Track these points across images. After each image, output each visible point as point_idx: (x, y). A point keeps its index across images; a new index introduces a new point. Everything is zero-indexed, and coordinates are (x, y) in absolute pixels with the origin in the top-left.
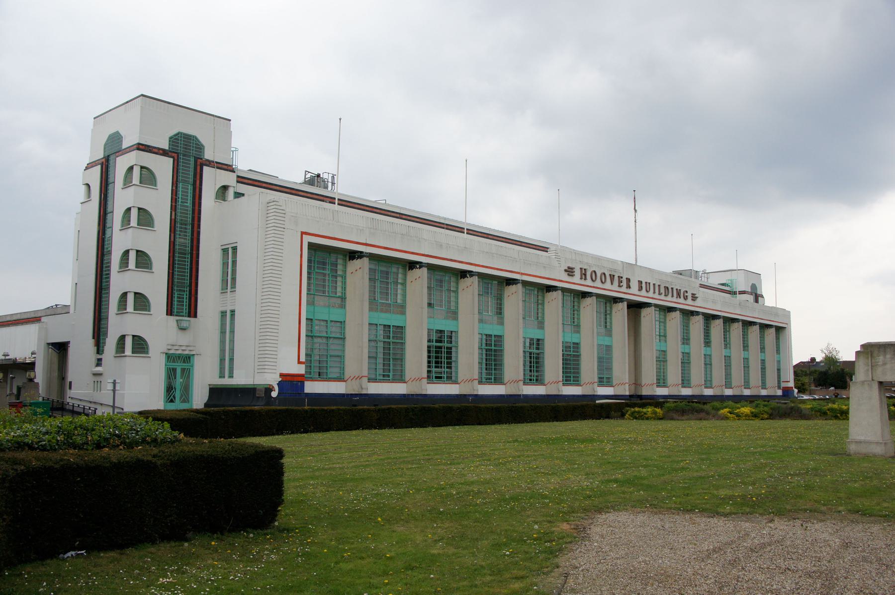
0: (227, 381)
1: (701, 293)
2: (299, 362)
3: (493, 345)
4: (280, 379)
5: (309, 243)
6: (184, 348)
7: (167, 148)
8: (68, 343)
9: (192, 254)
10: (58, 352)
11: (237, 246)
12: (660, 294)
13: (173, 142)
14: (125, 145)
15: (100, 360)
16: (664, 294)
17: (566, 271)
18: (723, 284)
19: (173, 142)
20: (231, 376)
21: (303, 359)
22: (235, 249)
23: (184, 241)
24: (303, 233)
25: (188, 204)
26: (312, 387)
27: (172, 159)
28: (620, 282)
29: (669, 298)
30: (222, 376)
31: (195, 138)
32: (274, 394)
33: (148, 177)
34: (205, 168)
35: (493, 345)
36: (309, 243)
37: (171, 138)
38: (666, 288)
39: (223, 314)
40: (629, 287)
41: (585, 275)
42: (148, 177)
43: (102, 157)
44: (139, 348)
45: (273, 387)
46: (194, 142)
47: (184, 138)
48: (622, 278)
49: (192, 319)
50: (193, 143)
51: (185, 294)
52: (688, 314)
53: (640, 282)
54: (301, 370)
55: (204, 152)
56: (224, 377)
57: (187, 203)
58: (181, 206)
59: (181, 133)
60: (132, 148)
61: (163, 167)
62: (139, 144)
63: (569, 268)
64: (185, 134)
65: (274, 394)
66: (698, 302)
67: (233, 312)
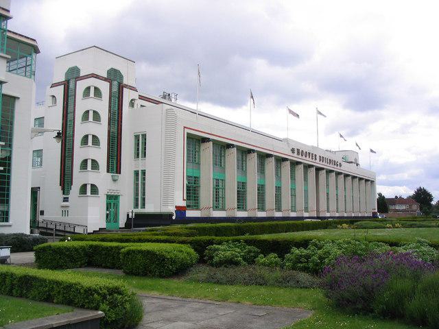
5: (188, 134)
9: (118, 137)
12: (312, 159)
20: (143, 206)
23: (115, 130)
24: (185, 127)
26: (190, 214)
28: (312, 156)
29: (331, 165)
36: (188, 134)
38: (330, 160)
39: (137, 173)
40: (316, 159)
42: (98, 92)
52: (338, 174)
54: (183, 204)
61: (104, 87)
67: (144, 173)
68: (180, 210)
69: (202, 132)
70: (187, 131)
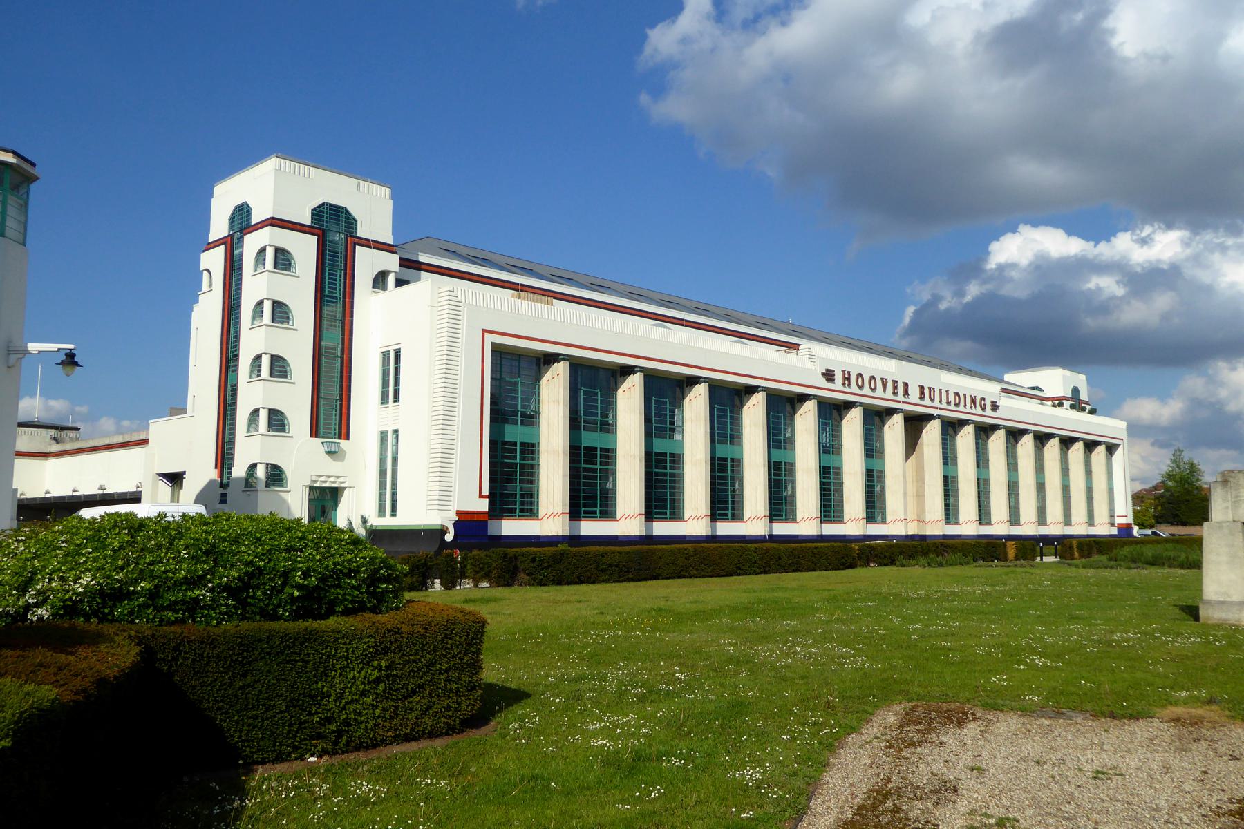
0: (387, 522)
1: (1005, 402)
2: (481, 496)
3: (668, 467)
4: (457, 518)
5: (493, 344)
6: (332, 479)
7: (308, 222)
8: (184, 473)
9: (342, 359)
10: (170, 485)
11: (400, 349)
13: (316, 215)
14: (255, 220)
15: (224, 496)
16: (953, 403)
17: (823, 374)
18: (1033, 388)
19: (316, 215)
21: (486, 491)
22: (398, 353)
24: (484, 331)
25: (337, 295)
27: (316, 237)
28: (895, 388)
30: (381, 512)
31: (345, 211)
32: (449, 537)
33: (283, 260)
34: (357, 246)
35: (668, 467)
36: (493, 344)
37: (313, 210)
38: (957, 394)
40: (906, 393)
41: (849, 379)
42: (283, 260)
43: (227, 234)
44: (274, 480)
45: (447, 528)
46: (344, 215)
47: (330, 209)
48: (897, 382)
49: (343, 443)
50: (327, 214)
51: (334, 411)
53: (922, 388)
55: (356, 229)
56: (384, 516)
57: (336, 293)
58: (328, 297)
59: (327, 204)
60: (266, 223)
61: (304, 249)
62: (273, 218)
63: (827, 370)
64: (332, 205)
65: (449, 537)
66: (999, 414)
67: (396, 432)
68: (468, 524)
69: (715, 370)
70: (490, 338)
